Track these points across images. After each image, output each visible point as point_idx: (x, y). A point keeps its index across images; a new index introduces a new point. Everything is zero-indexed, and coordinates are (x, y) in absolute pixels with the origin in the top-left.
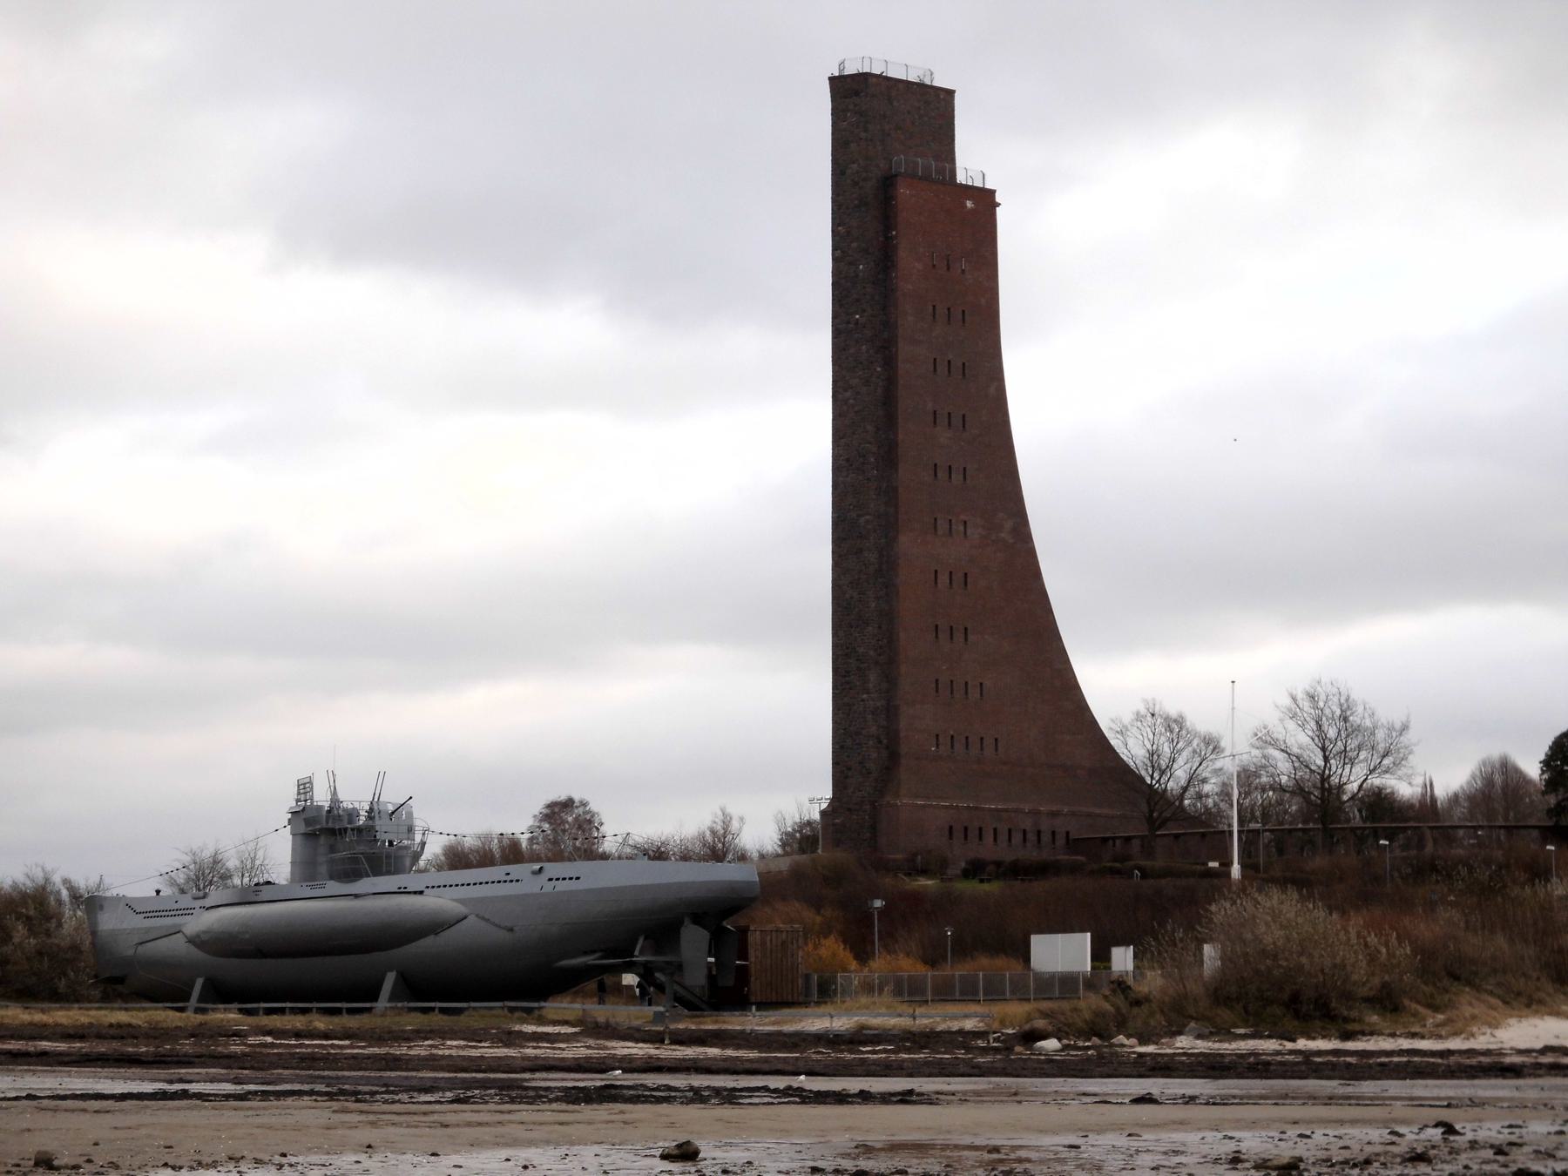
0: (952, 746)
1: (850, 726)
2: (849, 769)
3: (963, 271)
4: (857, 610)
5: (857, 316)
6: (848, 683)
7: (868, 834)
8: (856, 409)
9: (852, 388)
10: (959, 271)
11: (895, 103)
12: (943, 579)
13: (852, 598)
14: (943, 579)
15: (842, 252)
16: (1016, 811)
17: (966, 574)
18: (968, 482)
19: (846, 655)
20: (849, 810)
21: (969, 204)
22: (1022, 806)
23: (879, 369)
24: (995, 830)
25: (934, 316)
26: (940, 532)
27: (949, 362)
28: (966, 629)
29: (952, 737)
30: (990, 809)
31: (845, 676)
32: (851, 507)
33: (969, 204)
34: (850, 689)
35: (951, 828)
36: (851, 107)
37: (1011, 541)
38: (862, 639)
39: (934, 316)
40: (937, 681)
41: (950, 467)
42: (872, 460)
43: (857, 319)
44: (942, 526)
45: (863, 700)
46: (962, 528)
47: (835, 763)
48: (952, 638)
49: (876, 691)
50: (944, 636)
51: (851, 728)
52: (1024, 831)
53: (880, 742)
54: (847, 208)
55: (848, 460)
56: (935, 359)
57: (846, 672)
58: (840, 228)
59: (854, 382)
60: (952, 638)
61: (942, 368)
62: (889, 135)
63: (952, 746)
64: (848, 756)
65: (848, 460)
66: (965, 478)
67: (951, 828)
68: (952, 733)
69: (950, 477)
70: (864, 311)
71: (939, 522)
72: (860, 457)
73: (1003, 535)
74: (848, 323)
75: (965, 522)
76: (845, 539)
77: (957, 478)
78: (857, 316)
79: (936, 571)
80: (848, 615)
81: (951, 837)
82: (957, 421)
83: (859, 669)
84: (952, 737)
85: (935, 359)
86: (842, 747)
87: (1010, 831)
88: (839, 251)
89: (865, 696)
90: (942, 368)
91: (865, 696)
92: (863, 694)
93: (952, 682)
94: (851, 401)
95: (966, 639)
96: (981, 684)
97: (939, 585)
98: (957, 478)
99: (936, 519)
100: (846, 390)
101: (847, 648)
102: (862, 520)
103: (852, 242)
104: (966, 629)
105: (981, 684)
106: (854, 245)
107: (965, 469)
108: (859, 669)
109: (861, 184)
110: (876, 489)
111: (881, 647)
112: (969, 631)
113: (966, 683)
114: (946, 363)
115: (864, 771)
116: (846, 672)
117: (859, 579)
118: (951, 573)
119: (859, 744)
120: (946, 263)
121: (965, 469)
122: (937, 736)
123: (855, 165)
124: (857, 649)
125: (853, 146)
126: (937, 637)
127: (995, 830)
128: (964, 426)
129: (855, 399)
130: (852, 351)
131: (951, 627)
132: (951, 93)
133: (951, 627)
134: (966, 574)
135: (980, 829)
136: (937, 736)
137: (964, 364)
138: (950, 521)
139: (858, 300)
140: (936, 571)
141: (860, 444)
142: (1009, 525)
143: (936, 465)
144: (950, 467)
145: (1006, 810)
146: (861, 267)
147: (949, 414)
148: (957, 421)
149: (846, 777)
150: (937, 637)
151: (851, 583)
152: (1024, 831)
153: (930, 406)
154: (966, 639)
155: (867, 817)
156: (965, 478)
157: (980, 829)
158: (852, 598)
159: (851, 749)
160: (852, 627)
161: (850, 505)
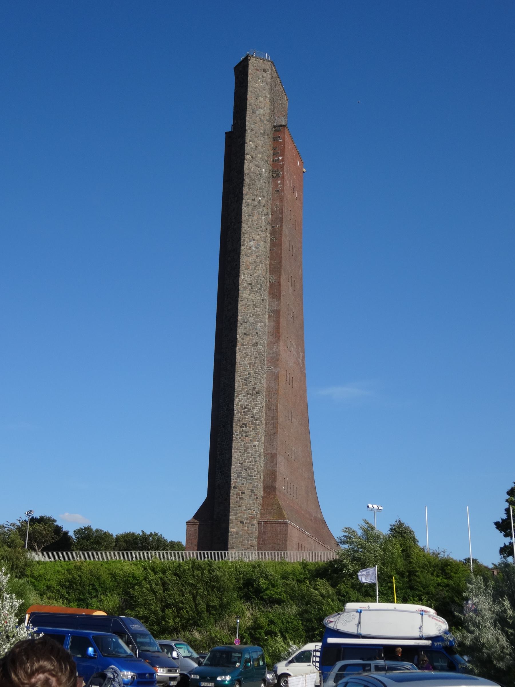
1: (245, 462)
2: (243, 493)
4: (253, 383)
5: (260, 198)
6: (245, 432)
8: (257, 254)
9: (254, 240)
13: (250, 374)
19: (244, 412)
31: (241, 427)
34: (247, 436)
36: (261, 76)
38: (256, 404)
43: (260, 200)
45: (255, 446)
51: (246, 464)
54: (256, 133)
55: (250, 284)
57: (244, 424)
59: (257, 237)
64: (243, 484)
65: (250, 284)
70: (264, 197)
72: (258, 284)
74: (254, 200)
76: (245, 334)
91: (256, 443)
92: (255, 441)
94: (254, 249)
100: (250, 241)
101: (245, 408)
103: (259, 153)
106: (260, 156)
108: (252, 424)
115: (253, 496)
116: (244, 424)
117: (255, 363)
119: (251, 476)
123: (262, 110)
124: (252, 410)
125: (261, 99)
129: (256, 248)
130: (256, 218)
139: (260, 189)
141: (259, 276)
146: (263, 170)
149: (241, 498)
151: (249, 364)
158: (250, 374)
161: (251, 313)
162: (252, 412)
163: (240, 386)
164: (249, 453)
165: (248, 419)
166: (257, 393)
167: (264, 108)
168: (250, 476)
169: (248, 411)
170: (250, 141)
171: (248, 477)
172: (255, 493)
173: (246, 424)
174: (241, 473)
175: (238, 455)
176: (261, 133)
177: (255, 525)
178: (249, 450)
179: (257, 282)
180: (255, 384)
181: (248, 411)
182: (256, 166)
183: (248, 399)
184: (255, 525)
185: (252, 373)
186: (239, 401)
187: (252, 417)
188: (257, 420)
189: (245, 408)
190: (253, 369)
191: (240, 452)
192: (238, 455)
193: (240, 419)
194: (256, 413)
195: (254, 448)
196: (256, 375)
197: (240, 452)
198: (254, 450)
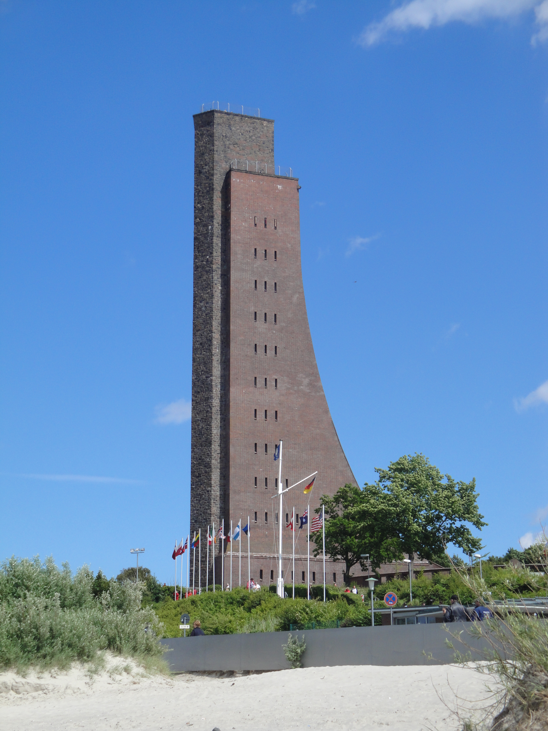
3: (276, 228)
4: (205, 435)
9: (204, 300)
10: (273, 228)
11: (233, 128)
12: (261, 415)
13: (203, 428)
14: (261, 415)
15: (200, 219)
17: (276, 412)
25: (255, 255)
26: (258, 385)
27: (266, 282)
29: (266, 513)
31: (198, 477)
32: (203, 373)
35: (261, 571)
37: (308, 391)
38: (208, 453)
39: (255, 255)
40: (256, 478)
41: (266, 346)
43: (208, 259)
44: (260, 382)
45: (208, 491)
48: (266, 451)
50: (261, 449)
54: (203, 193)
55: (201, 344)
56: (256, 281)
58: (199, 205)
60: (266, 451)
61: (261, 287)
62: (229, 148)
65: (201, 344)
66: (276, 353)
67: (261, 571)
68: (266, 511)
69: (266, 352)
75: (276, 380)
77: (271, 352)
78: (208, 257)
79: (256, 410)
80: (200, 439)
82: (270, 317)
83: (206, 472)
84: (266, 513)
85: (256, 281)
86: (196, 521)
88: (198, 219)
89: (209, 489)
90: (261, 287)
91: (209, 489)
93: (266, 479)
97: (258, 418)
98: (271, 352)
99: (255, 378)
100: (201, 302)
101: (200, 459)
103: (205, 212)
107: (276, 347)
109: (210, 177)
114: (264, 283)
117: (207, 416)
118: (266, 411)
121: (276, 347)
122: (256, 513)
126: (256, 451)
130: (204, 278)
131: (266, 445)
133: (266, 445)
134: (276, 412)
136: (256, 513)
137: (275, 283)
138: (266, 379)
140: (256, 410)
141: (208, 333)
142: (306, 381)
143: (256, 345)
144: (266, 346)
147: (265, 314)
148: (270, 317)
150: (256, 451)
153: (252, 309)
156: (276, 353)
161: (202, 371)
162: (205, 461)
163: (195, 441)
165: (202, 469)
167: (209, 163)
168: (204, 519)
170: (198, 203)
171: (204, 521)
175: (195, 503)
176: (208, 191)
178: (204, 496)
179: (207, 339)
180: (208, 435)
182: (204, 226)
186: (194, 454)
187: (205, 466)
190: (205, 422)
191: (197, 500)
192: (195, 503)
196: (207, 427)
197: (197, 500)
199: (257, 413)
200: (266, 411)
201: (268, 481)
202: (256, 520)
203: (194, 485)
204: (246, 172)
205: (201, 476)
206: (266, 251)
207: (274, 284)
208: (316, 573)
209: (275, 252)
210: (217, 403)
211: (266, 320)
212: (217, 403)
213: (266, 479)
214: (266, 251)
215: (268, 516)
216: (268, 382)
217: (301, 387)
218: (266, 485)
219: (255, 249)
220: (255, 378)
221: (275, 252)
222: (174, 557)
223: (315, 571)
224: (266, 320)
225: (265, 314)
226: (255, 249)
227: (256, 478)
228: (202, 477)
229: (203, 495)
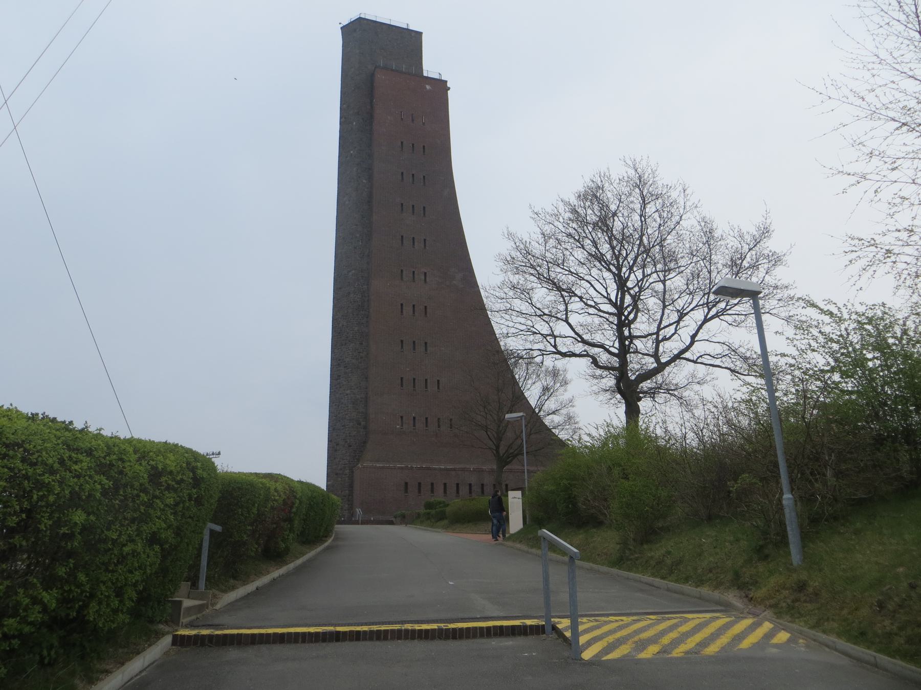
0: (414, 425)
1: (339, 413)
7: (347, 492)
12: (408, 310)
13: (343, 326)
14: (408, 310)
16: (463, 470)
17: (426, 307)
18: (427, 248)
20: (337, 474)
21: (428, 87)
22: (468, 467)
23: (364, 181)
24: (445, 484)
28: (426, 343)
29: (414, 418)
30: (440, 469)
31: (338, 379)
33: (428, 87)
34: (341, 387)
35: (406, 484)
37: (462, 286)
40: (402, 378)
41: (413, 238)
42: (358, 235)
45: (347, 395)
46: (423, 277)
47: (330, 441)
48: (414, 349)
49: (357, 388)
52: (470, 485)
53: (360, 424)
56: (402, 173)
60: (414, 349)
63: (414, 425)
67: (406, 484)
69: (414, 244)
71: (404, 272)
73: (454, 282)
74: (346, 157)
75: (425, 273)
76: (340, 288)
78: (352, 152)
79: (402, 305)
81: (406, 490)
85: (402, 173)
86: (334, 429)
87: (458, 485)
89: (348, 392)
91: (348, 392)
92: (347, 390)
93: (414, 379)
95: (426, 350)
96: (438, 381)
99: (402, 271)
101: (339, 360)
102: (350, 274)
104: (426, 343)
105: (438, 381)
110: (360, 254)
111: (362, 358)
112: (428, 345)
113: (426, 380)
117: (348, 312)
118: (414, 306)
120: (411, 118)
121: (425, 240)
122: (402, 417)
127: (445, 484)
128: (424, 214)
131: (414, 342)
132: (419, 34)
133: (414, 342)
134: (426, 307)
135: (432, 484)
136: (402, 417)
138: (414, 272)
143: (402, 237)
144: (413, 238)
145: (454, 470)
146: (354, 123)
147: (413, 206)
149: (336, 450)
152: (470, 485)
154: (426, 350)
155: (347, 479)
157: (432, 484)
159: (339, 429)
160: (342, 345)
162: (345, 361)
164: (342, 403)
166: (349, 341)
168: (343, 426)
169: (341, 362)
172: (347, 442)
173: (340, 376)
174: (335, 425)
177: (347, 475)
181: (341, 362)
183: (342, 350)
184: (347, 475)
185: (345, 324)
187: (345, 367)
188: (349, 368)
189: (339, 360)
193: (335, 373)
194: (348, 361)
195: (348, 397)
198: (346, 399)
199: (404, 308)
200: (414, 306)
201: (416, 381)
202: (402, 426)
203: (332, 389)
204: (392, 70)
205: (340, 379)
206: (413, 145)
207: (422, 177)
208: (473, 485)
209: (424, 147)
210: (358, 298)
211: (413, 213)
212: (358, 298)
213: (414, 379)
214: (413, 145)
215: (416, 421)
216: (416, 276)
217: (454, 282)
218: (414, 387)
219: (402, 143)
220: (402, 271)
221: (424, 147)
222: (219, 454)
223: (472, 483)
224: (413, 213)
225: (413, 206)
226: (402, 143)
227: (402, 378)
228: (341, 379)
229: (342, 399)
